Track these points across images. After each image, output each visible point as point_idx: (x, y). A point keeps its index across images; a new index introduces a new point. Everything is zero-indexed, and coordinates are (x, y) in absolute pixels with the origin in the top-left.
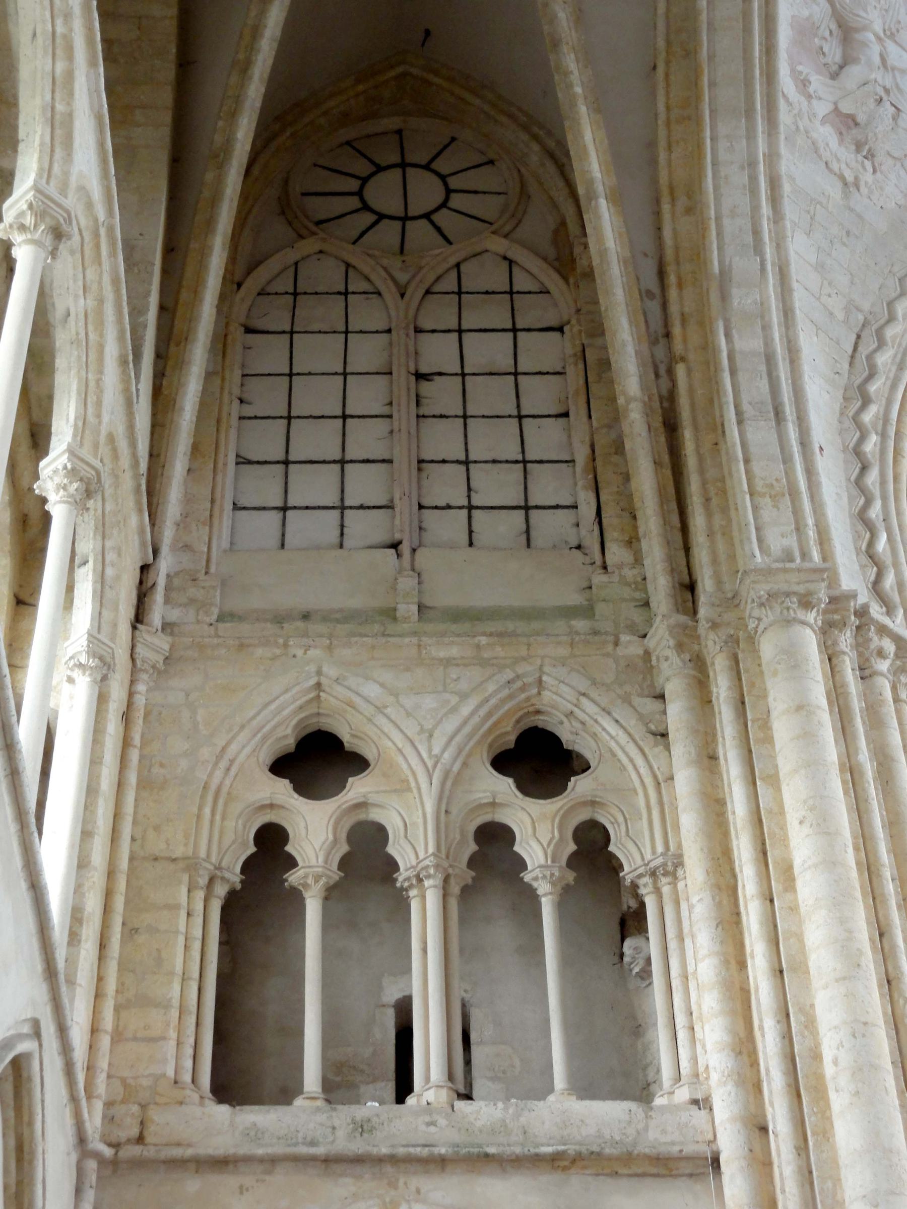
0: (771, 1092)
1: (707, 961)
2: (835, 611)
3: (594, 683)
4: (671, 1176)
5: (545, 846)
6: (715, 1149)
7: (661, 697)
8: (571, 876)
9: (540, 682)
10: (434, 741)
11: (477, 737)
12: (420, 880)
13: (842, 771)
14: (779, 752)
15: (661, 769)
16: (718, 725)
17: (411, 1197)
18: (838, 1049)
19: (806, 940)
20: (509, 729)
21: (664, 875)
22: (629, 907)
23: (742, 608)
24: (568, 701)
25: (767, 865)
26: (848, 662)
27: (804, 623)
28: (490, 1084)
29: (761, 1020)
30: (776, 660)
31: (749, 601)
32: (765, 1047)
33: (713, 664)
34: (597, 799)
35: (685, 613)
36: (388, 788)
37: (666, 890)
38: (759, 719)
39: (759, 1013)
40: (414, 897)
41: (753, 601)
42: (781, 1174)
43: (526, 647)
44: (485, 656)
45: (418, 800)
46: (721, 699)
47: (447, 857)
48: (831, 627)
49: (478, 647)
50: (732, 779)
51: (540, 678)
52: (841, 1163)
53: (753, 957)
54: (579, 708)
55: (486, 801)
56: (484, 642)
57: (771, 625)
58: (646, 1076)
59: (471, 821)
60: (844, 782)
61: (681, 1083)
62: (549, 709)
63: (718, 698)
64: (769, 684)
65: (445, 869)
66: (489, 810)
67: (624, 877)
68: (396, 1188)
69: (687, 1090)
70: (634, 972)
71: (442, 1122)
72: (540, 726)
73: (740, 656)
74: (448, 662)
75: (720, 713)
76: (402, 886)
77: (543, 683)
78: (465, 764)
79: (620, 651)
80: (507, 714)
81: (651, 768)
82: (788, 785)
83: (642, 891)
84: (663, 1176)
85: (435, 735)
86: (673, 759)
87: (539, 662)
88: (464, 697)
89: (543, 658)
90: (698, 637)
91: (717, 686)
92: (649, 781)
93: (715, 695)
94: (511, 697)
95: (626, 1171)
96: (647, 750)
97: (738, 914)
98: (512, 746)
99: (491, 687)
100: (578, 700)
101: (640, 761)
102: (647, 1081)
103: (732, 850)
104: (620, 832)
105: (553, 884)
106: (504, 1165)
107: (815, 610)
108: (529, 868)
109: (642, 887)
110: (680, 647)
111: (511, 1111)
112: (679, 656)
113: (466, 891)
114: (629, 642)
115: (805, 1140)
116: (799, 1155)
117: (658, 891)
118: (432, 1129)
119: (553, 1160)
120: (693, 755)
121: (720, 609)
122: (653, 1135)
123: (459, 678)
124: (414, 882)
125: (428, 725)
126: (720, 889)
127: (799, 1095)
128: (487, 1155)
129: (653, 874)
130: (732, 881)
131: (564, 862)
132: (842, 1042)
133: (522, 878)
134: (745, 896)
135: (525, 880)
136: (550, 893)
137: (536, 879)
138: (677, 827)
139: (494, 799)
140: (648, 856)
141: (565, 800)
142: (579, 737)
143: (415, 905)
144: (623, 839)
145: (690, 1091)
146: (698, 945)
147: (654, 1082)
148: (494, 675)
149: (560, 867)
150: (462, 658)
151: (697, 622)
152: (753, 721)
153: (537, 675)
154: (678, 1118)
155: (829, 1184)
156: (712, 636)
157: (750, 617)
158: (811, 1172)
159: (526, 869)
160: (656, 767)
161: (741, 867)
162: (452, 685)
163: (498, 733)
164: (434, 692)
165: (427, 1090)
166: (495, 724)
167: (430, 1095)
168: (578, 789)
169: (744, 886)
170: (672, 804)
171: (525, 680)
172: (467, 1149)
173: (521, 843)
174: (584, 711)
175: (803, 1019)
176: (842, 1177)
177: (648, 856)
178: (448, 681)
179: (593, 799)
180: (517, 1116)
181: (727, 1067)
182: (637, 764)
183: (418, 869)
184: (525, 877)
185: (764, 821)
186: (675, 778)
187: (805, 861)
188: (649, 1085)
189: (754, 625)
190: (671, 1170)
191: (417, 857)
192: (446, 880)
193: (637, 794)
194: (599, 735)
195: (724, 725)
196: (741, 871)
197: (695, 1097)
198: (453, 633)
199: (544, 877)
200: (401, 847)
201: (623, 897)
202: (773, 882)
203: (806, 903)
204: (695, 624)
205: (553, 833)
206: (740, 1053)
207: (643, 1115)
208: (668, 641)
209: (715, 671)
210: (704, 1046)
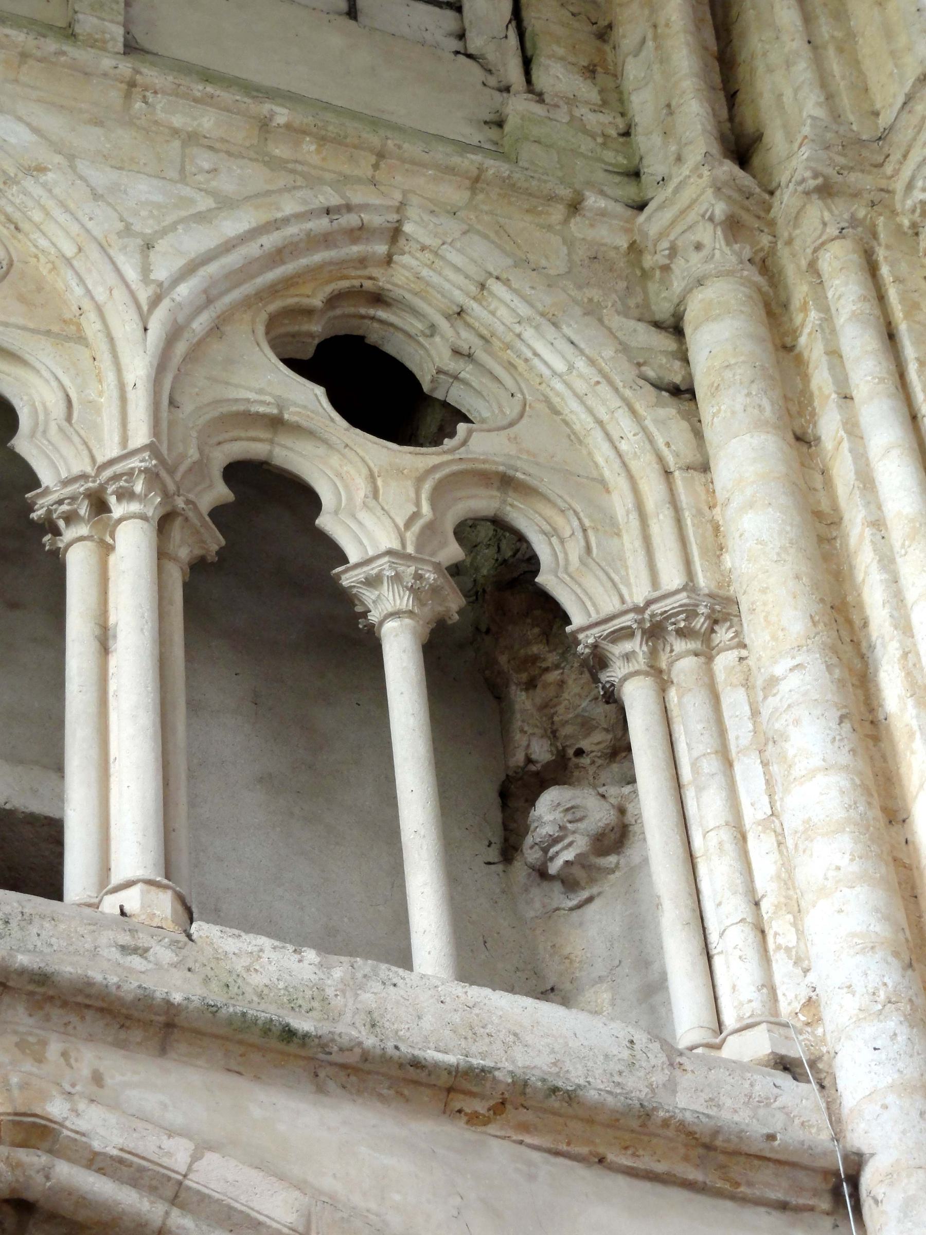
4: (733, 1197)
9: (395, 234)
11: (248, 289)
12: (100, 506)
15: (673, 447)
17: (78, 1088)
20: (317, 302)
22: (529, 760)
36: (31, 325)
43: (373, 159)
44: (277, 152)
55: (262, 409)
68: (40, 1060)
71: (165, 955)
72: (373, 338)
74: (192, 138)
78: (216, 329)
79: (577, 227)
80: (313, 272)
84: (719, 1194)
87: (398, 196)
88: (226, 204)
94: (326, 240)
95: (626, 1161)
106: (322, 1074)
111: (338, 973)
114: (603, 213)
118: (136, 962)
119: (450, 1090)
121: (841, 160)
128: (289, 1034)
130: (858, 665)
136: (410, 613)
145: (771, 1039)
153: (394, 217)
154: (747, 1085)
160: (660, 442)
163: (291, 301)
166: (289, 282)
180: (354, 986)
181: (885, 984)
184: (343, 577)
201: (518, 736)
204: (767, 196)
205: (418, 504)
206: (910, 965)
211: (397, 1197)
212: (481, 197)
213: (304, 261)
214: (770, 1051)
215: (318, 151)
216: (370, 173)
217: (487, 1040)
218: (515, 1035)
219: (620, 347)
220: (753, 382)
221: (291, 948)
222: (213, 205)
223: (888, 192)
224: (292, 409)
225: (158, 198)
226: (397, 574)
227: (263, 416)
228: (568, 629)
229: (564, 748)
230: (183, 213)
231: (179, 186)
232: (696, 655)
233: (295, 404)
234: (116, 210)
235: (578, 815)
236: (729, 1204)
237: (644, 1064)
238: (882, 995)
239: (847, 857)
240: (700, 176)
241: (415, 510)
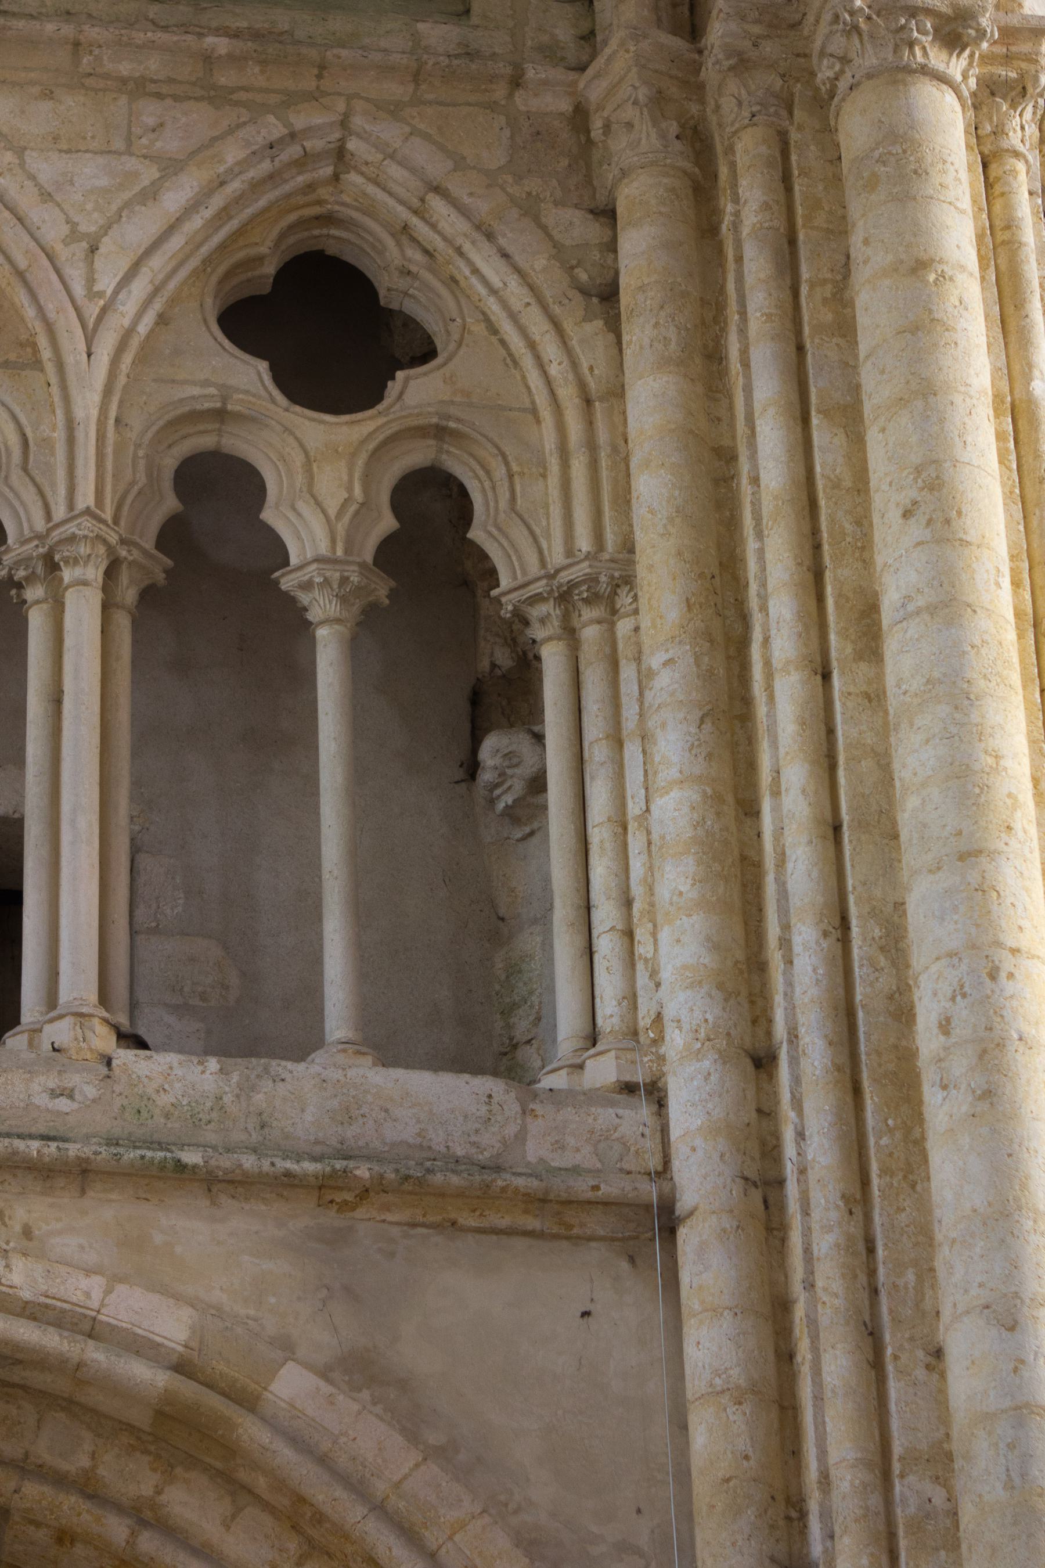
0: (796, 1080)
1: (675, 794)
2: (1008, 59)
3: (460, 164)
4: (568, 1238)
5: (332, 512)
6: (666, 1187)
7: (608, 215)
8: (382, 590)
9: (340, 154)
10: (99, 263)
11: (194, 263)
12: (52, 566)
13: (998, 413)
14: (867, 357)
15: (596, 372)
16: (731, 287)
17: (12, 1244)
18: (953, 999)
19: (896, 766)
20: (263, 250)
21: (586, 601)
22: (494, 666)
23: (806, 32)
24: (402, 202)
25: (820, 598)
26: (1023, 177)
27: (942, 79)
28: (170, 1019)
29: (786, 927)
30: (876, 154)
31: (827, 17)
32: (790, 984)
33: (730, 150)
34: (452, 425)
35: (675, 31)
37: (590, 634)
38: (824, 282)
39: (784, 911)
40: (37, 602)
41: (837, 18)
42: (807, 1250)
43: (315, 71)
44: (223, 81)
45: (55, 390)
46: (745, 231)
47: (116, 520)
48: (993, 94)
49: (208, 59)
50: (757, 406)
51: (342, 141)
52: (939, 1237)
53: (776, 793)
54: (423, 219)
55: (207, 405)
56: (223, 51)
57: (869, 76)
58: (509, 1027)
59: (170, 446)
60: (1000, 436)
61: (599, 1047)
62: (356, 215)
63: (736, 226)
64: (855, 208)
65: (110, 549)
66: (210, 427)
67: (497, 601)
69: (614, 1062)
70: (501, 806)
72: (331, 251)
73: (794, 136)
75: (739, 259)
76: (10, 577)
77: (348, 157)
78: (162, 320)
81: (574, 364)
82: (883, 430)
83: (538, 632)
84: (556, 1237)
85: (102, 250)
86: (628, 352)
87: (341, 106)
89: (350, 98)
90: (701, 87)
91: (736, 200)
92: (567, 393)
93: (727, 220)
95: (473, 1222)
96: (568, 326)
97: (747, 701)
98: (267, 289)
99: (232, 154)
100: (422, 200)
101: (551, 350)
102: (511, 1039)
103: (743, 560)
104: (496, 502)
105: (343, 599)
106: (214, 1189)
107: (967, 52)
108: (294, 560)
109: (536, 624)
110: (659, 101)
112: (655, 123)
113: (148, 595)
114: (545, 83)
115: (865, 1182)
116: (851, 1213)
117: (570, 634)
118: (63, 1104)
120: (673, 346)
121: (756, 29)
122: (535, 1150)
123: (162, 125)
124: (40, 570)
125: (88, 226)
126: (711, 641)
127: (857, 1090)
128: (180, 1167)
129: (564, 597)
131: (368, 555)
132: (962, 987)
133: (277, 582)
134: (767, 663)
135: (283, 587)
136: (338, 621)
137: (307, 586)
138: (624, 500)
139: (224, 399)
140: (557, 557)
141: (384, 420)
142: (417, 284)
143: (37, 621)
144: (502, 516)
145: (618, 1066)
146: (657, 759)
147: (529, 1042)
148: (239, 126)
149: (363, 565)
150: (171, 81)
151: (700, 52)
152: (812, 286)
153: (337, 135)
154: (590, 1121)
155: (910, 1276)
156: (733, 86)
157: (822, 54)
158: (871, 1250)
159: (286, 562)
160: (585, 366)
161: (764, 599)
162: (144, 141)
163: (240, 255)
164: (102, 153)
165: (52, 1021)
167: (61, 1032)
168: (412, 397)
169: (766, 641)
170: (615, 449)
171: (308, 144)
172: (139, 1152)
173: (277, 506)
174: (433, 226)
175: (877, 932)
176: (939, 1264)
177: (557, 557)
178: (137, 130)
179: (444, 423)
180: (246, 1089)
181: (706, 1020)
182: (543, 355)
183: (50, 541)
184: (282, 581)
185: (822, 502)
186: (630, 394)
187: (908, 598)
188: (515, 1047)
189: (830, 74)
190: (570, 1227)
191: (48, 515)
192: (111, 573)
193: (538, 421)
194: (463, 283)
195: (747, 286)
196: (764, 608)
197: (627, 1078)
198: (153, 22)
199: (327, 581)
200: (11, 488)
202: (833, 637)
203: (904, 687)
204: (696, 56)
205: (350, 489)
207: (516, 1108)
208: (635, 88)
209: (733, 166)
210: (654, 973)
211: (273, 1300)
212: (423, 87)
213: (249, 211)
214: (614, 1079)
215: (262, 72)
216: (314, 84)
217: (361, 1120)
218: (387, 1111)
219: (554, 251)
220: (662, 307)
221: (195, 1059)
222: (157, 175)
223: (805, 56)
224: (236, 396)
225: (103, 182)
226: (326, 580)
227: (208, 411)
228: (494, 593)
229: (525, 653)
230: (127, 195)
231: (125, 158)
232: (599, 622)
233: (238, 390)
234: (62, 210)
235: (515, 761)
236: (565, 1244)
237: (499, 1118)
238: (702, 1035)
239: (689, 881)
240: (627, 51)
241: (346, 496)
